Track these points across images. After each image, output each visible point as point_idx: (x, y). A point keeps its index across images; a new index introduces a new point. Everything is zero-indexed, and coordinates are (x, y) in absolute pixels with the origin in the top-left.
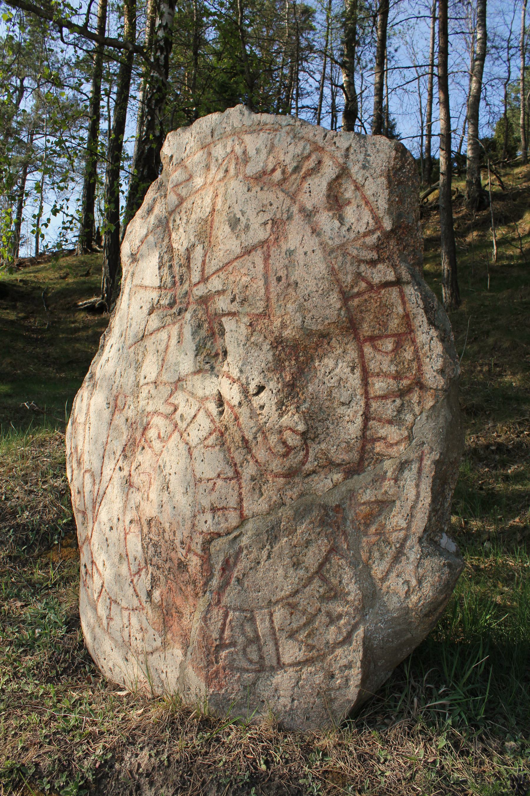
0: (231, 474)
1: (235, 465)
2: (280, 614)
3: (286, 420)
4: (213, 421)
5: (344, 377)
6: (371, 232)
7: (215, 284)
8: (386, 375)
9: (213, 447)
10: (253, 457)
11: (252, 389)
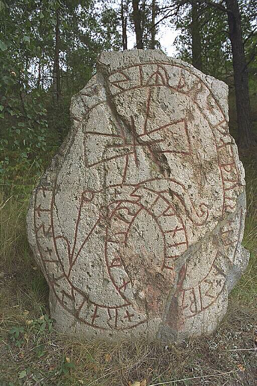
2: (203, 284)
3: (202, 201)
4: (168, 203)
5: (216, 181)
6: (223, 121)
7: (157, 136)
8: (229, 180)
11: (187, 187)
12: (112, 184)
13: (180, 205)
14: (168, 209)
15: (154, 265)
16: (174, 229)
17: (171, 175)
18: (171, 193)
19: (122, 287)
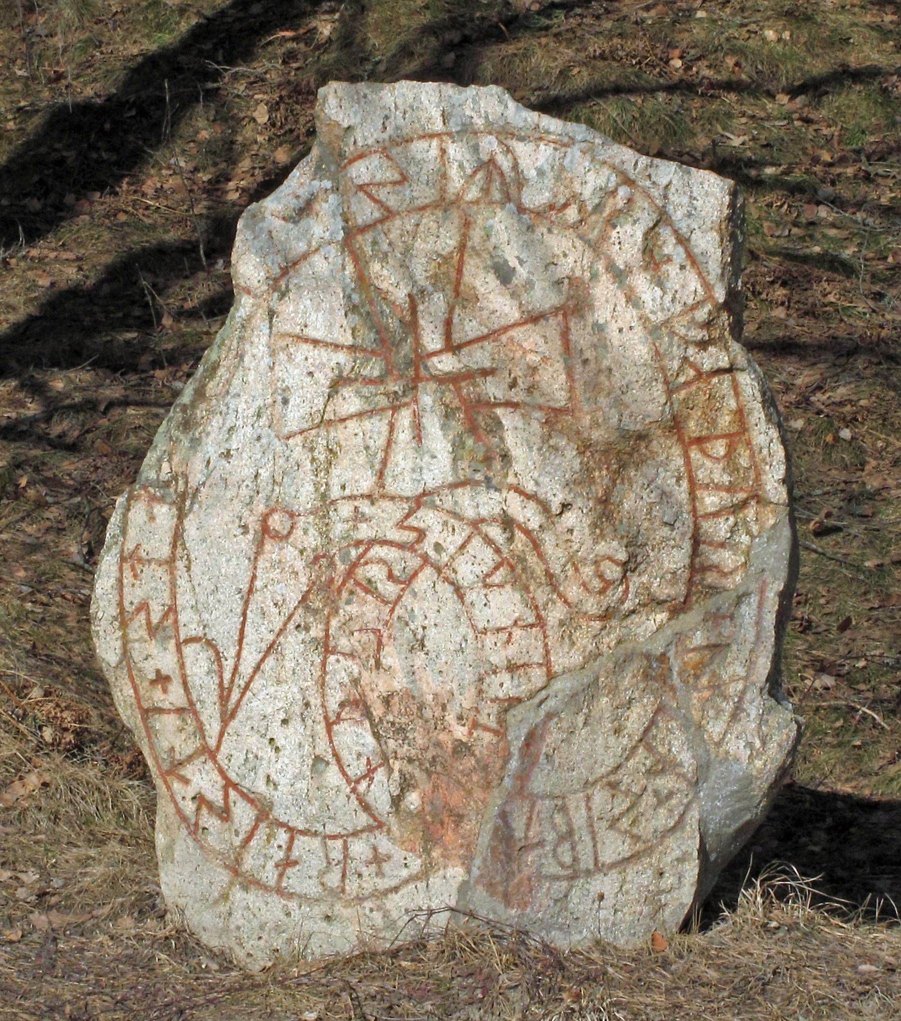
0: (532, 620)
1: (536, 607)
3: (602, 548)
4: (498, 551)
9: (501, 586)
10: (560, 595)
11: (555, 508)
12: (347, 492)
13: (532, 559)
14: (496, 568)
15: (451, 718)
16: (510, 623)
17: (511, 473)
18: (508, 523)
19: (364, 777)
